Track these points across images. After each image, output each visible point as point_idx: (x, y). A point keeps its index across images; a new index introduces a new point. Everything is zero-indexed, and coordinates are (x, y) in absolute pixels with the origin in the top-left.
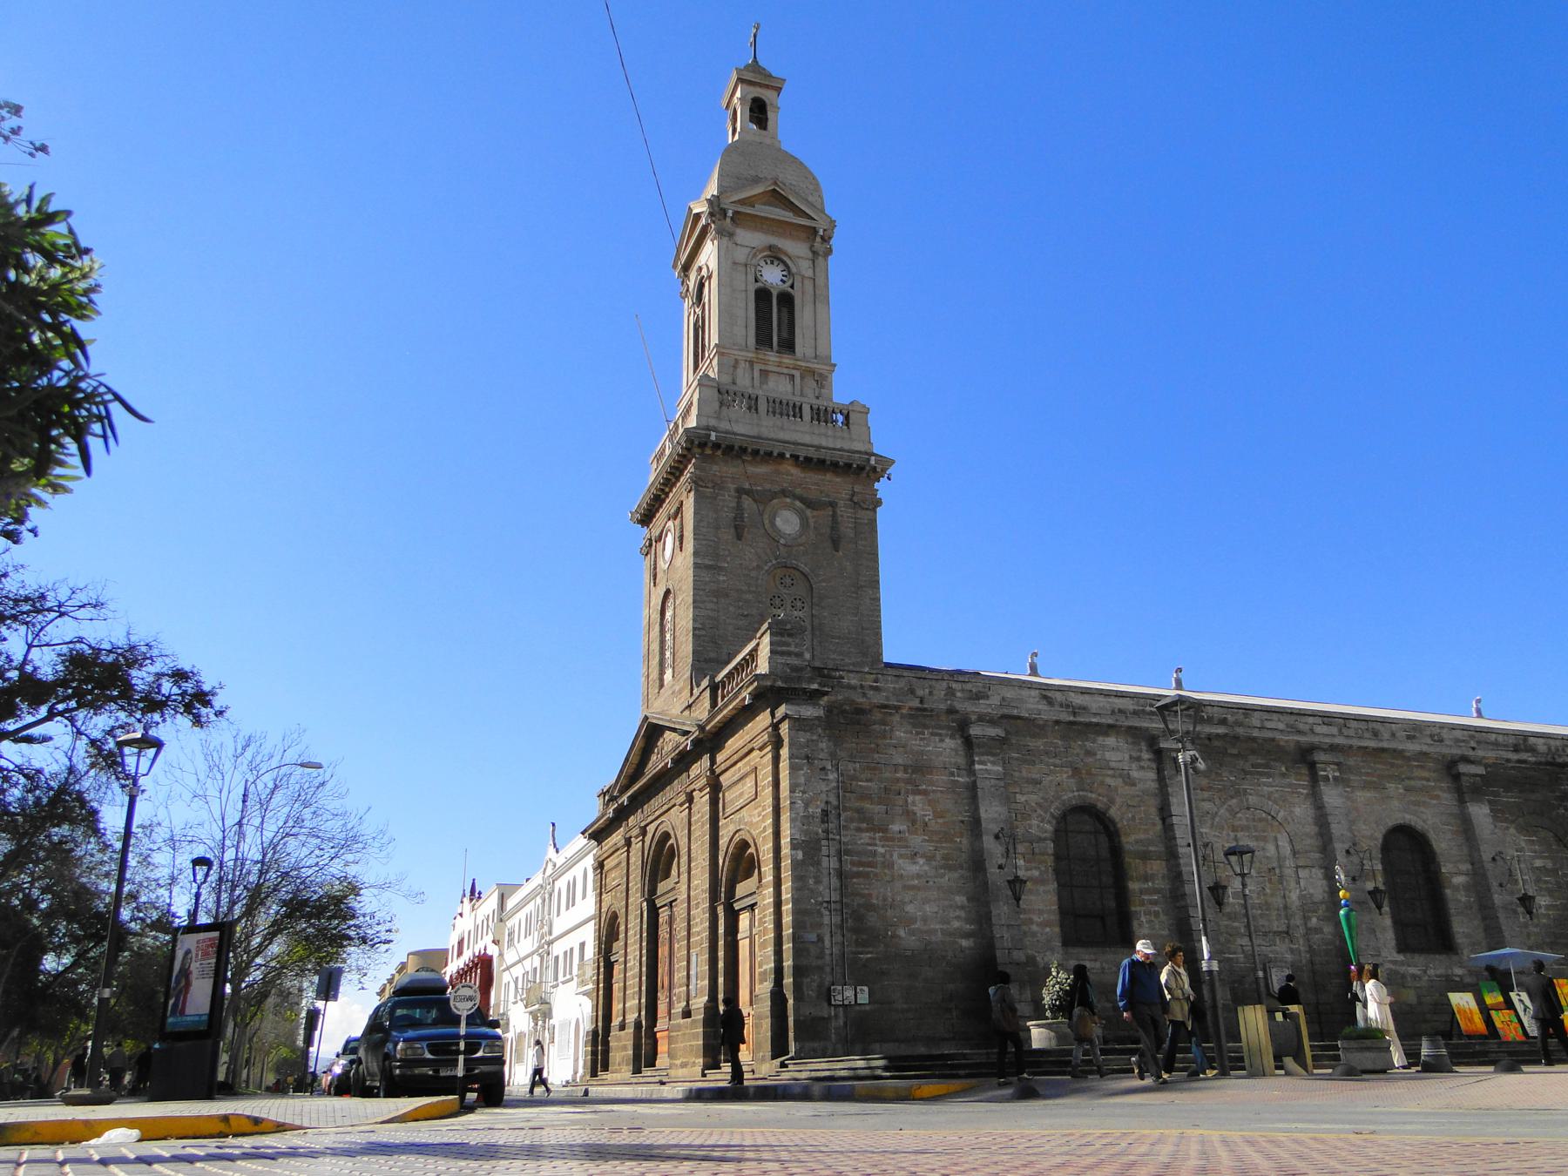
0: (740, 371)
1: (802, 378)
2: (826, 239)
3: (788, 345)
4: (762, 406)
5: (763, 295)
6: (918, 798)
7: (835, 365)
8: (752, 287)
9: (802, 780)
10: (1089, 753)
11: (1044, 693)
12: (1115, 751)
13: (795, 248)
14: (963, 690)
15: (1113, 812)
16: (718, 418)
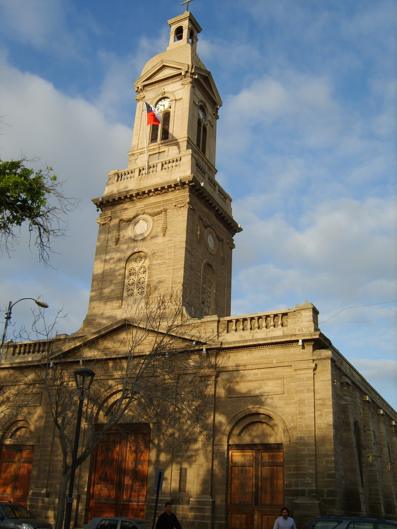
3: (204, 151)
11: (350, 368)
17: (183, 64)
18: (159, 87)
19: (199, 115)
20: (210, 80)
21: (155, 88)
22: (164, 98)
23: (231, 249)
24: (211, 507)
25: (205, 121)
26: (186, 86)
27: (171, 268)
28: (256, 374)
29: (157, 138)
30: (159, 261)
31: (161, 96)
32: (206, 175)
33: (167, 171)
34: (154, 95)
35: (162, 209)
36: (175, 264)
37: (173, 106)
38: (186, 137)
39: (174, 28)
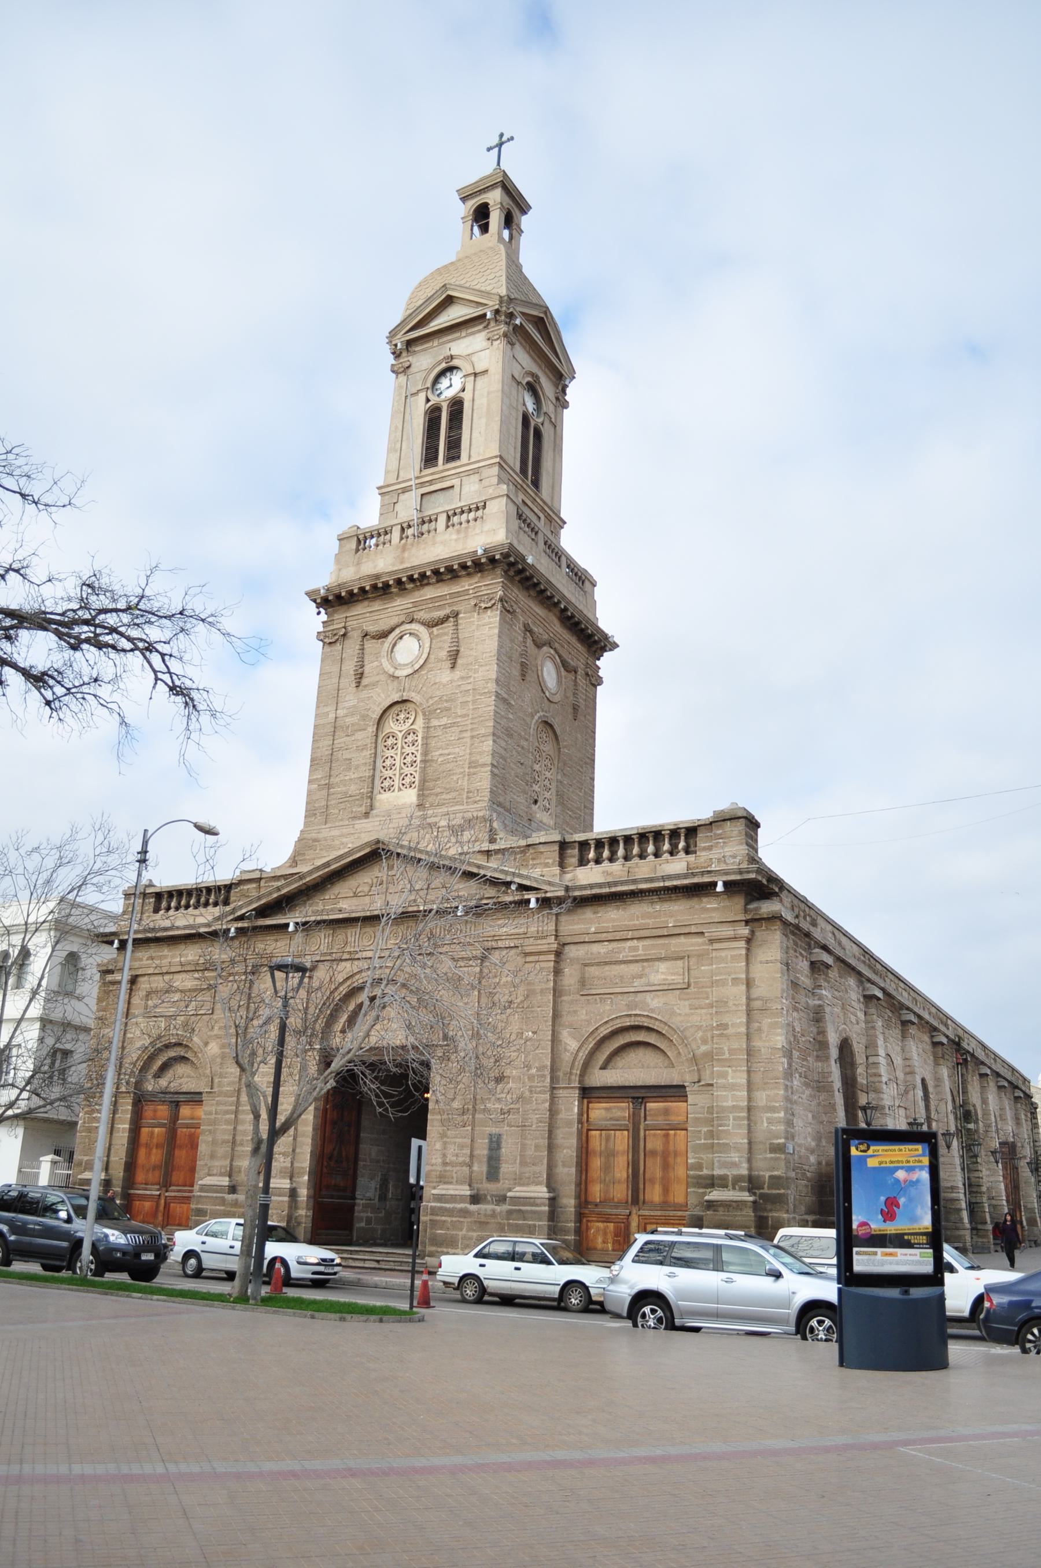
3: (536, 483)
8: (521, 409)
13: (547, 387)
17: (487, 294)
18: (440, 344)
19: (524, 404)
21: (432, 347)
22: (451, 369)
23: (595, 686)
25: (538, 416)
26: (496, 343)
27: (468, 734)
28: (636, 949)
29: (436, 458)
30: (444, 721)
31: (444, 365)
32: (540, 534)
33: (458, 532)
34: (429, 361)
35: (447, 611)
36: (474, 726)
37: (469, 387)
38: (496, 457)
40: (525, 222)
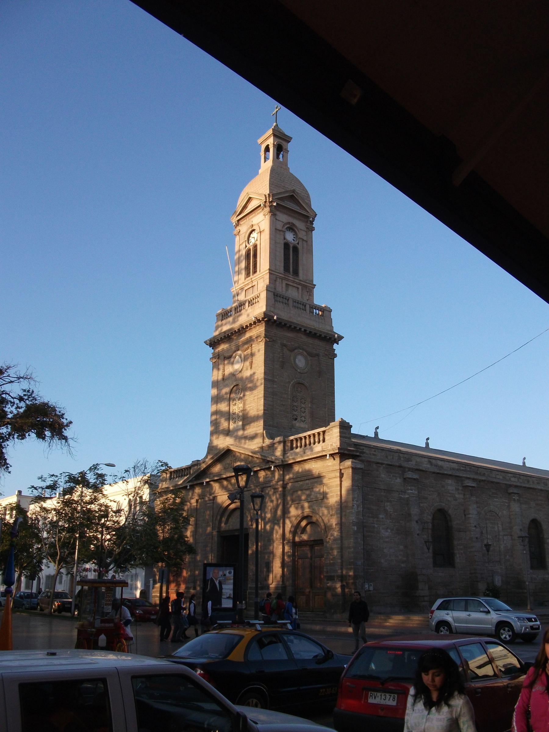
0: (277, 283)
1: (302, 289)
2: (312, 223)
3: (296, 273)
4: (291, 302)
5: (286, 245)
6: (388, 504)
7: (315, 285)
8: (282, 242)
9: (356, 496)
10: (443, 487)
11: (430, 460)
12: (450, 485)
13: (300, 225)
14: (403, 457)
15: (450, 512)
16: (274, 308)
20: (296, 197)
24: (254, 591)
27: (256, 398)
31: (251, 230)
36: (258, 394)
39: (263, 147)
40: (290, 146)
